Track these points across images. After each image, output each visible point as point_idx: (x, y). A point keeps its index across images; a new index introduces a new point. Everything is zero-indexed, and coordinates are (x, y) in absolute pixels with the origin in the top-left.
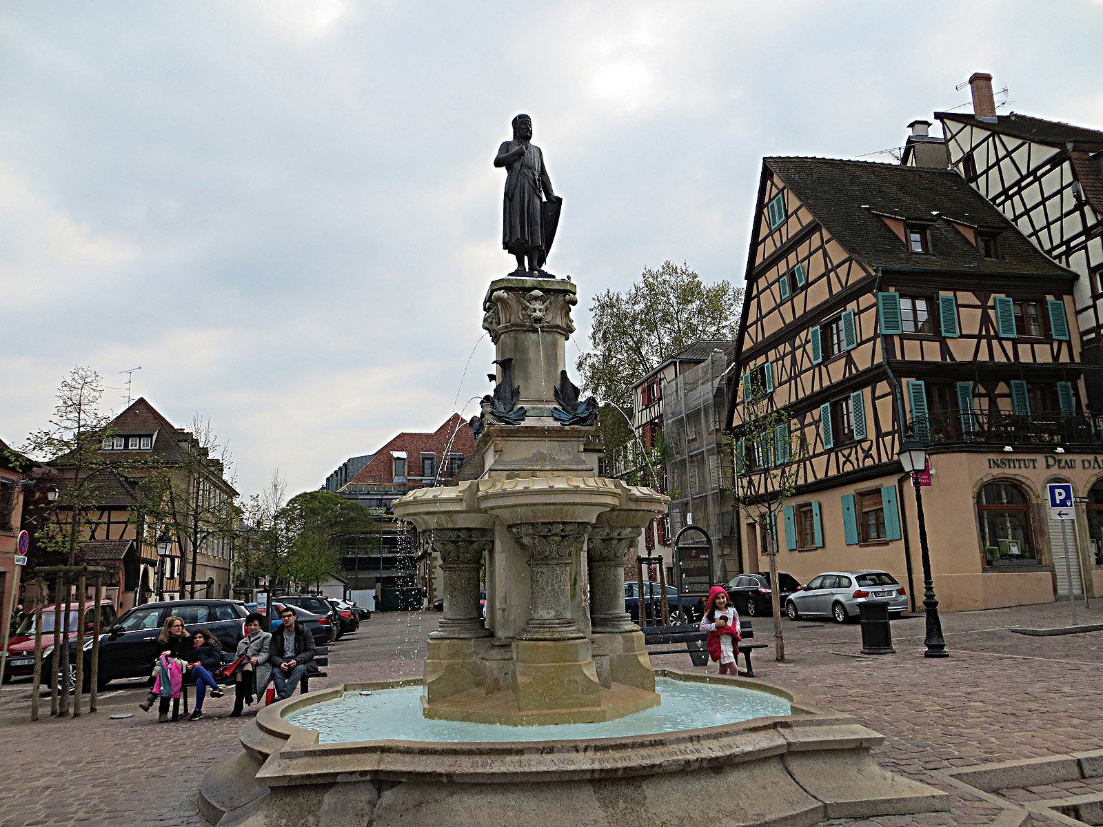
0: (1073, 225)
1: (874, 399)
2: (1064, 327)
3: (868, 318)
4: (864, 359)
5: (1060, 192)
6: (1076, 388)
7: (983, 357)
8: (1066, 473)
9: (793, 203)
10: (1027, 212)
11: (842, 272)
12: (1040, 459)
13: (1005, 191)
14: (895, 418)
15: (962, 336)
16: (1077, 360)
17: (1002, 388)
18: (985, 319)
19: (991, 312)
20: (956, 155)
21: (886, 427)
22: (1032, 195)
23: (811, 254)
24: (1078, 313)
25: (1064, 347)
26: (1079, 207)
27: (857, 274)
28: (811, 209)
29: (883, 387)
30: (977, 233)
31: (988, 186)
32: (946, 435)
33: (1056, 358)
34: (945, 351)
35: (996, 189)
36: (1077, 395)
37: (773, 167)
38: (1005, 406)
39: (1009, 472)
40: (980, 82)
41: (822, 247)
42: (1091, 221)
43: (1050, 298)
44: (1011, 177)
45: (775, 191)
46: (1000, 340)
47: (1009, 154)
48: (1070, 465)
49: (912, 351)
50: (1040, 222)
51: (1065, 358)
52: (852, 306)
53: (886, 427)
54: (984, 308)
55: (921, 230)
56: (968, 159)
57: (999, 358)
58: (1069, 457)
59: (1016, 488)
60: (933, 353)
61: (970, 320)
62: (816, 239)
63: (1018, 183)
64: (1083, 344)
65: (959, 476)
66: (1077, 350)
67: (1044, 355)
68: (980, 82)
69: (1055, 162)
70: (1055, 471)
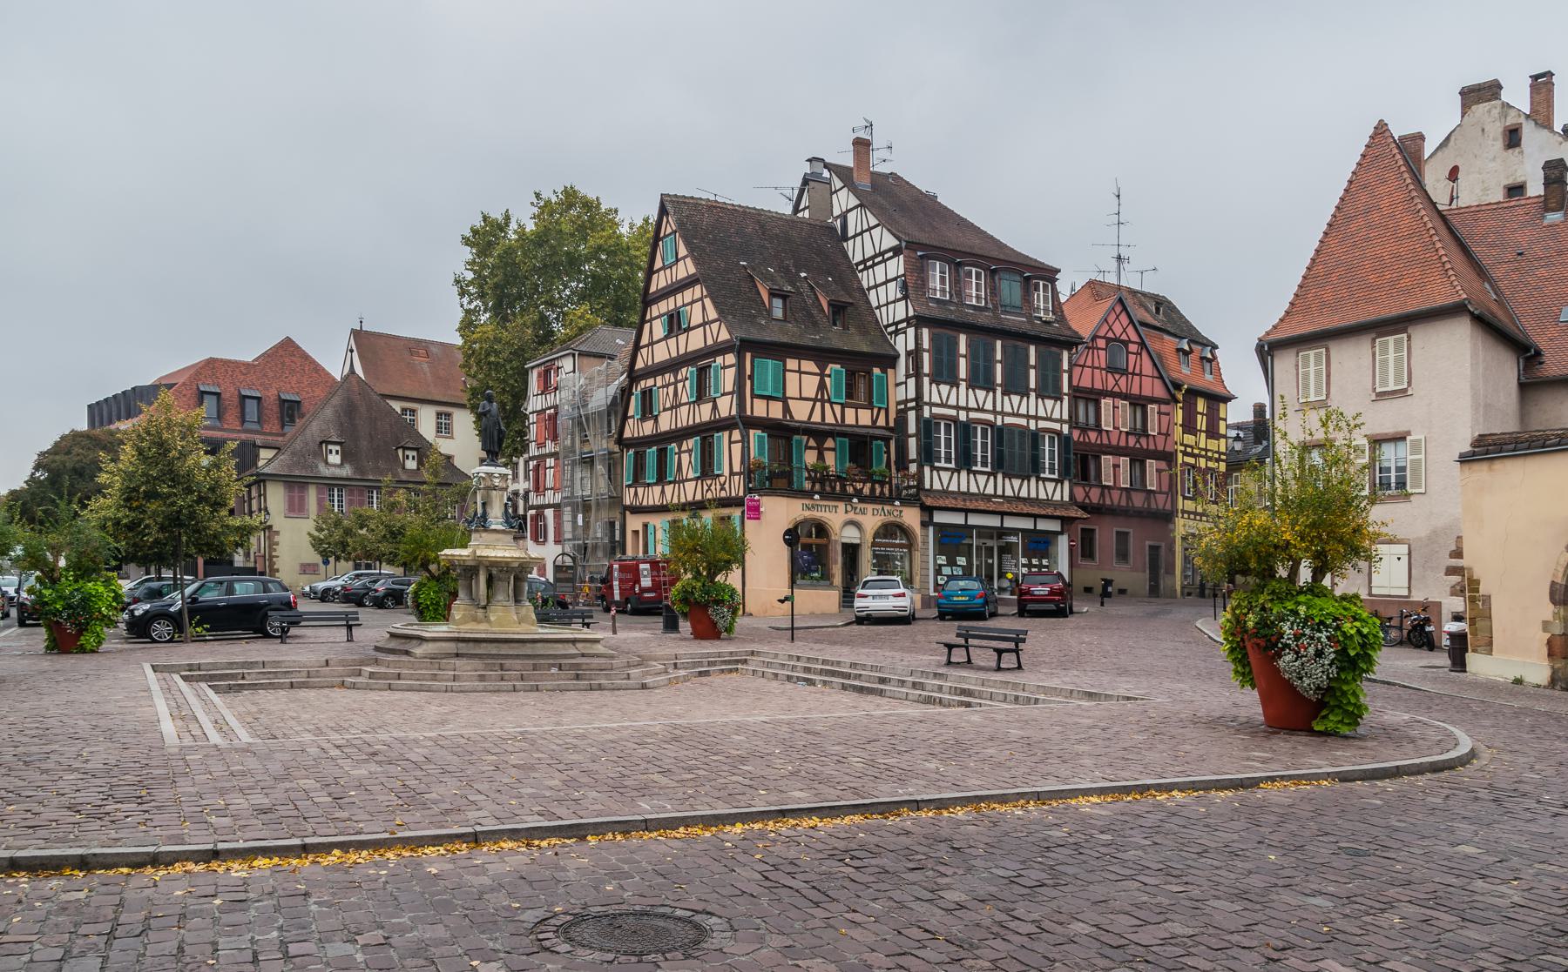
0: (900, 311)
1: (730, 442)
2: (884, 396)
3: (730, 374)
4: (726, 407)
5: (895, 279)
6: (888, 447)
7: (817, 418)
8: (859, 518)
9: (683, 251)
10: (876, 286)
11: (715, 326)
12: (841, 506)
13: (864, 261)
14: (742, 462)
15: (801, 398)
16: (892, 424)
17: (829, 443)
18: (822, 386)
19: (827, 380)
20: (836, 212)
21: (736, 468)
22: (879, 273)
23: (693, 302)
24: (897, 385)
25: (883, 413)
26: (905, 297)
27: (724, 335)
28: (696, 262)
29: (736, 435)
30: (830, 304)
31: (857, 251)
32: (776, 478)
33: (874, 422)
34: (786, 409)
35: (858, 258)
36: (888, 452)
37: (669, 207)
38: (830, 459)
39: (817, 514)
40: (862, 146)
41: (701, 299)
42: (911, 313)
43: (876, 371)
44: (869, 253)
45: (669, 230)
46: (832, 404)
47: (870, 229)
48: (863, 512)
49: (759, 409)
50: (883, 301)
51: (881, 422)
52: (719, 360)
53: (736, 468)
54: (822, 375)
55: (784, 297)
56: (844, 217)
57: (830, 419)
58: (862, 506)
59: (821, 529)
60: (776, 411)
61: (810, 385)
62: (698, 291)
63: (873, 258)
64: (898, 412)
65: (780, 512)
66: (892, 415)
67: (865, 417)
68: (862, 146)
69: (896, 251)
70: (851, 516)
